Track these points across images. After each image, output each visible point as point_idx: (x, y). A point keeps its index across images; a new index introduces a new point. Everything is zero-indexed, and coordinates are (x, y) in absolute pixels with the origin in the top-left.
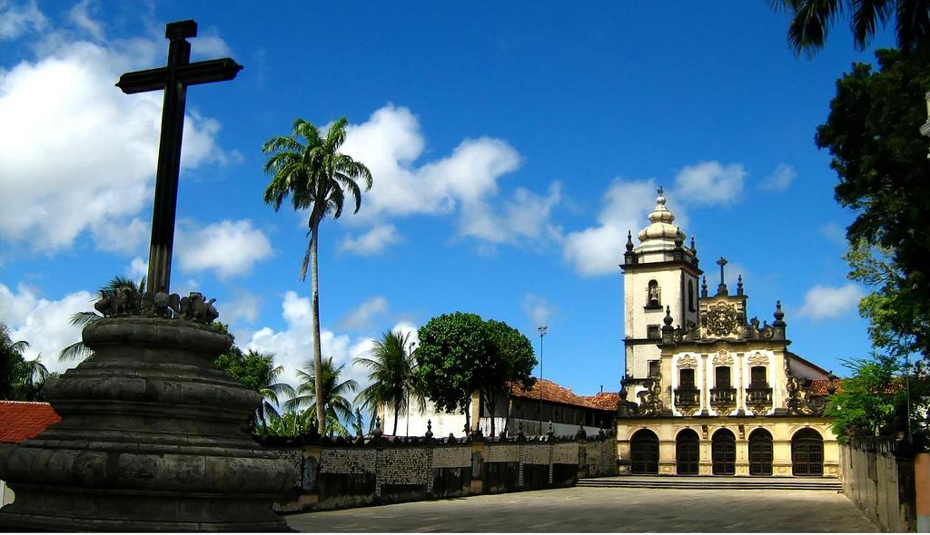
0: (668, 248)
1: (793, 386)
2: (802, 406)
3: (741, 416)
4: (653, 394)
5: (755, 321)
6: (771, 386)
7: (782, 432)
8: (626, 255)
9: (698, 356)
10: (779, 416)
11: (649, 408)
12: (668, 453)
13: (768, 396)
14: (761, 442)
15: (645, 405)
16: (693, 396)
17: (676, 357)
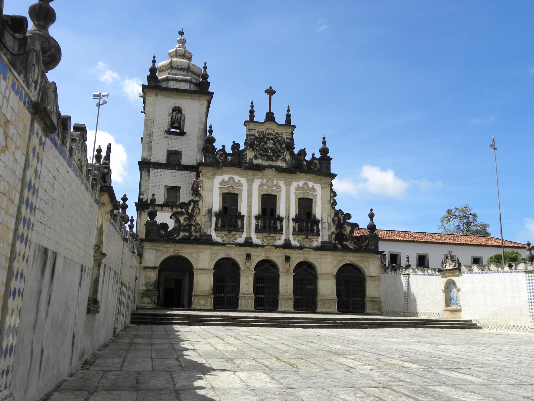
0: (194, 81)
1: (339, 220)
2: (347, 240)
3: (287, 245)
4: (191, 216)
5: (303, 153)
6: (319, 216)
7: (327, 265)
8: (149, 78)
9: (243, 181)
10: (324, 247)
11: (183, 231)
12: (203, 282)
13: (315, 228)
14: (306, 275)
15: (178, 228)
16: (236, 222)
17: (218, 179)
